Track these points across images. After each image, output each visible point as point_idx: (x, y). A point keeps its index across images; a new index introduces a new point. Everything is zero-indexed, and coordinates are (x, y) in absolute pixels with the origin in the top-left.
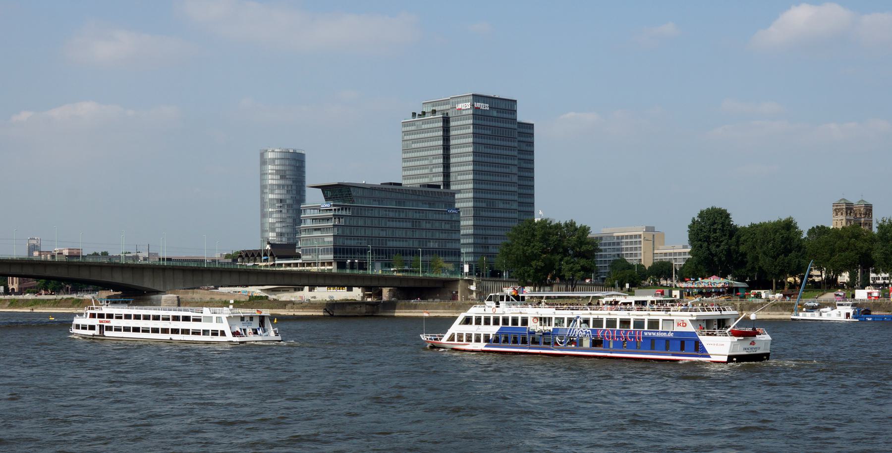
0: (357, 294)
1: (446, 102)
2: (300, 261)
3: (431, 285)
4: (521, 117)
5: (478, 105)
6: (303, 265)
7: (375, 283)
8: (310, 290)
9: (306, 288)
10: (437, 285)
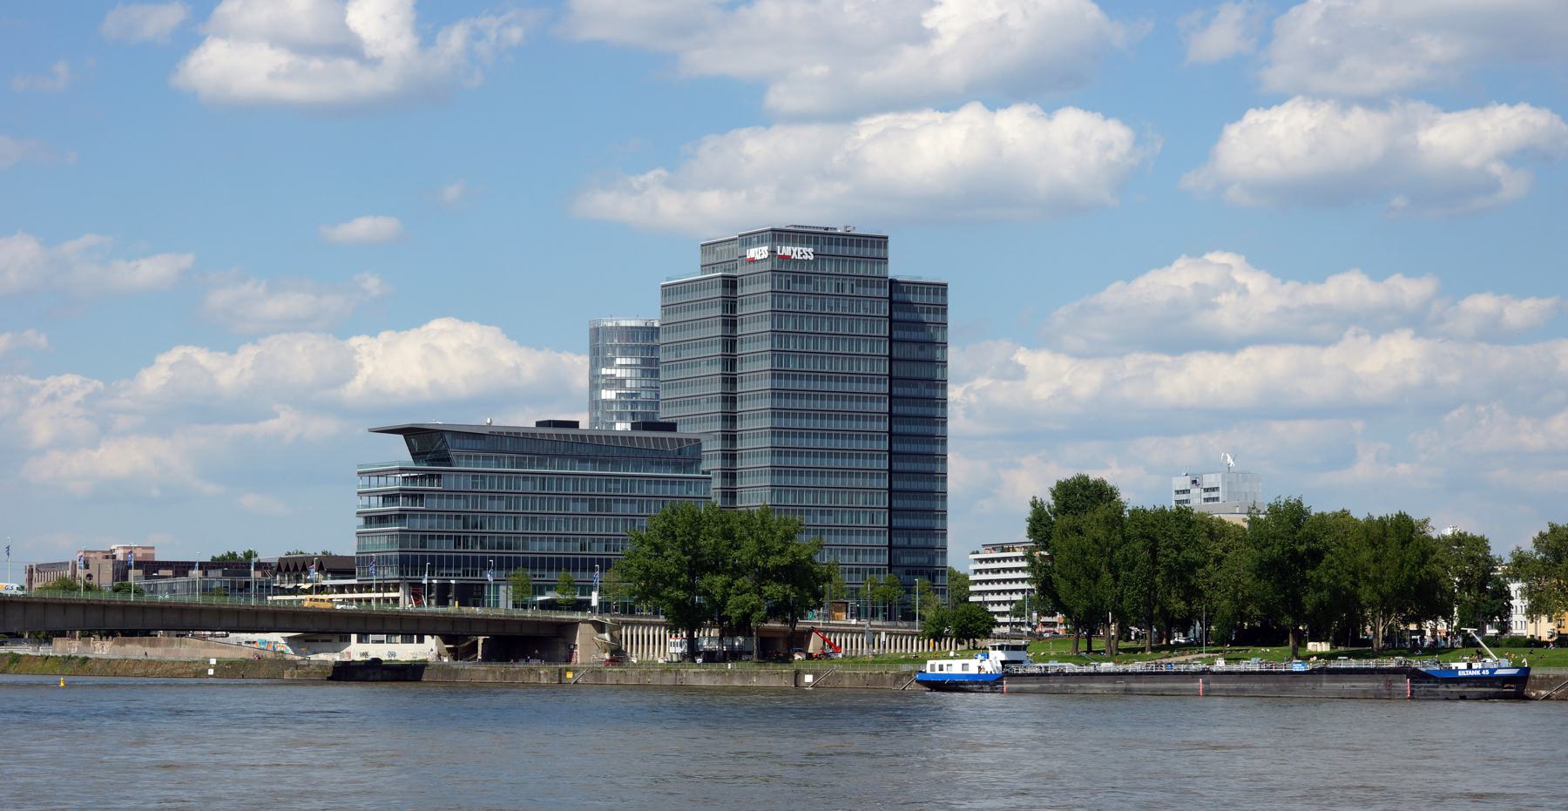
2: (354, 582)
5: (786, 250)
6: (360, 588)
7: (460, 630)
8: (359, 641)
9: (354, 637)
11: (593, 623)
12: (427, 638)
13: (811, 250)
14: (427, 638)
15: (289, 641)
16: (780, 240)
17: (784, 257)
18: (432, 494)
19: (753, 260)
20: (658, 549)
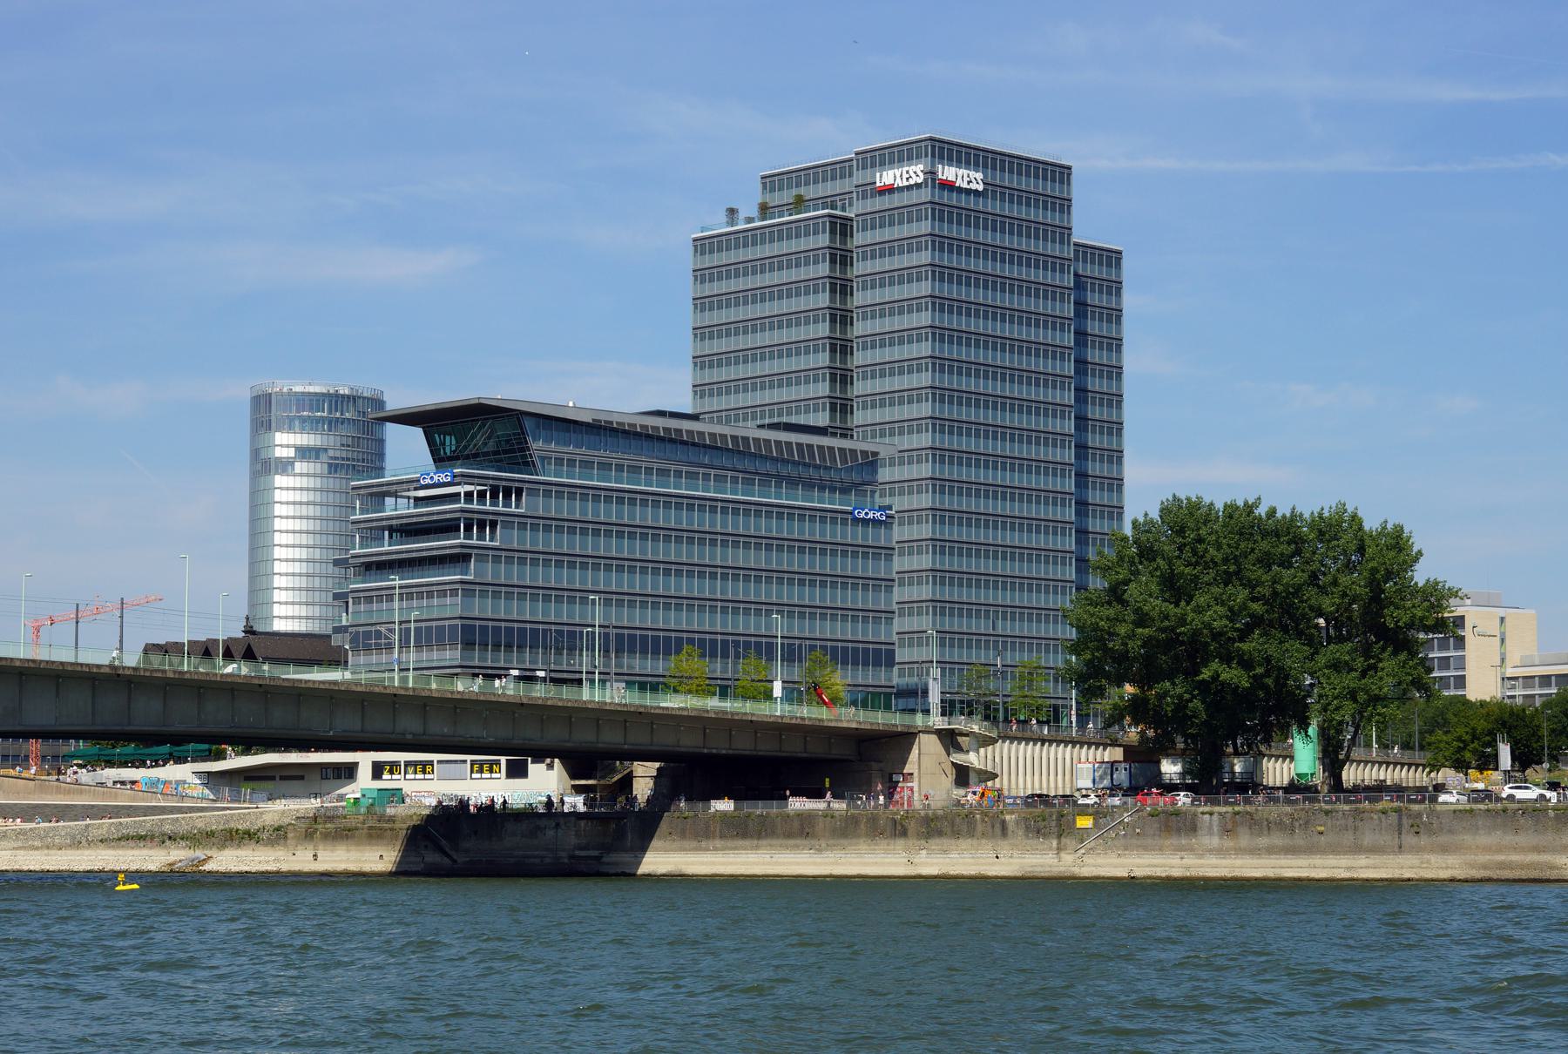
0: (545, 783)
1: (839, 169)
3: (817, 749)
4: (1086, 229)
5: (949, 173)
10: (836, 752)
11: (939, 732)
12: (535, 769)
13: (979, 176)
14: (535, 769)
15: (211, 779)
16: (941, 158)
17: (948, 186)
18: (509, 521)
19: (889, 190)
20: (1175, 588)
